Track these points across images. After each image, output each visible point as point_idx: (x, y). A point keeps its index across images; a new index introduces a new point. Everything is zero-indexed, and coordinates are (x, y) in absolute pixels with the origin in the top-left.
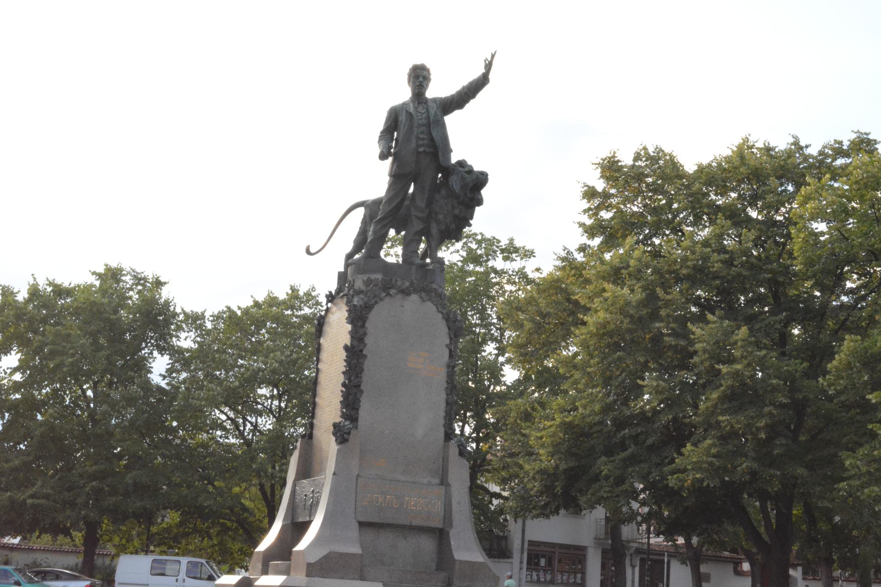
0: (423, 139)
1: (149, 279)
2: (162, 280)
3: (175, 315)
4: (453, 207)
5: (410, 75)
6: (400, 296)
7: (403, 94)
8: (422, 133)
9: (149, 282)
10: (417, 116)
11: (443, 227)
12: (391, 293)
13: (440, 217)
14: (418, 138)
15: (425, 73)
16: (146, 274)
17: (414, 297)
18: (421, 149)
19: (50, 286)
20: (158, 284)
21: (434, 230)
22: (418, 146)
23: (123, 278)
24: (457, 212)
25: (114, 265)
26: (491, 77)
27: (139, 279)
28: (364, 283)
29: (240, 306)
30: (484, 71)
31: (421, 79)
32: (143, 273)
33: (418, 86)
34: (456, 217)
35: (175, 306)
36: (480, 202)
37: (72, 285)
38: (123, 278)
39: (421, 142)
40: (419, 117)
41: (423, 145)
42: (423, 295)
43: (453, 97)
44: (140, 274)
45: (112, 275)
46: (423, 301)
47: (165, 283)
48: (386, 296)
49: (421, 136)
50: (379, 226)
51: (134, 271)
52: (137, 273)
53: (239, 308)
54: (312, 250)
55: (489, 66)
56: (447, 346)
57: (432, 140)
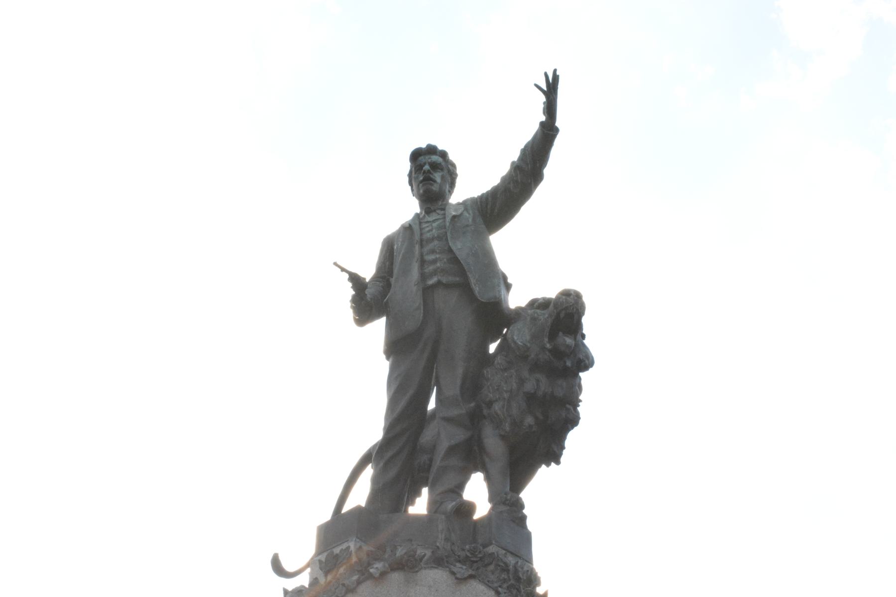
0: (434, 261)
4: (522, 381)
5: (411, 178)
6: (396, 577)
8: (433, 252)
10: (421, 229)
11: (507, 427)
12: (372, 570)
13: (497, 408)
14: (423, 262)
15: (435, 158)
17: (437, 576)
18: (431, 282)
21: (493, 443)
22: (423, 277)
24: (529, 387)
26: (558, 124)
28: (321, 569)
30: (543, 118)
31: (427, 167)
33: (421, 182)
34: (531, 398)
36: (585, 362)
39: (430, 269)
40: (427, 229)
41: (434, 273)
42: (461, 570)
43: (498, 184)
46: (461, 580)
48: (359, 583)
49: (431, 257)
50: (381, 464)
54: (289, 567)
55: (550, 109)
57: (455, 260)
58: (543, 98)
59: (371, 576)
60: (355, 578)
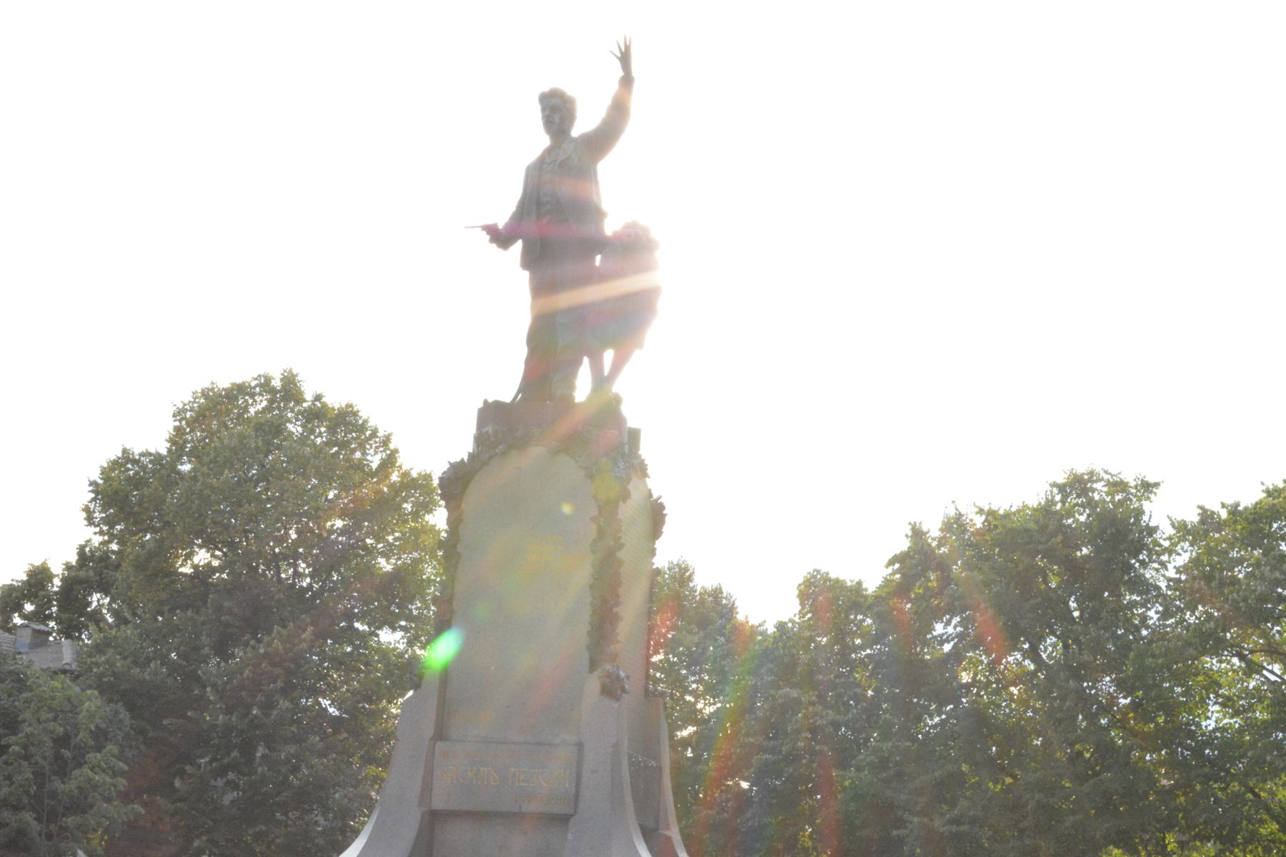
1: (1128, 483)
2: (1151, 480)
3: (1151, 531)
7: (543, 141)
9: (1131, 487)
16: (1122, 476)
19: (981, 514)
20: (1147, 487)
23: (1095, 486)
25: (1081, 469)
27: (1118, 486)
29: (1225, 502)
32: (1119, 474)
35: (1151, 516)
37: (1013, 509)
38: (1095, 486)
44: (1116, 476)
45: (1078, 485)
47: (1157, 485)
48: (490, 458)
51: (1106, 472)
52: (1112, 476)
53: (1223, 506)
56: (593, 519)
58: (618, 65)
59: (496, 454)
60: (488, 455)
